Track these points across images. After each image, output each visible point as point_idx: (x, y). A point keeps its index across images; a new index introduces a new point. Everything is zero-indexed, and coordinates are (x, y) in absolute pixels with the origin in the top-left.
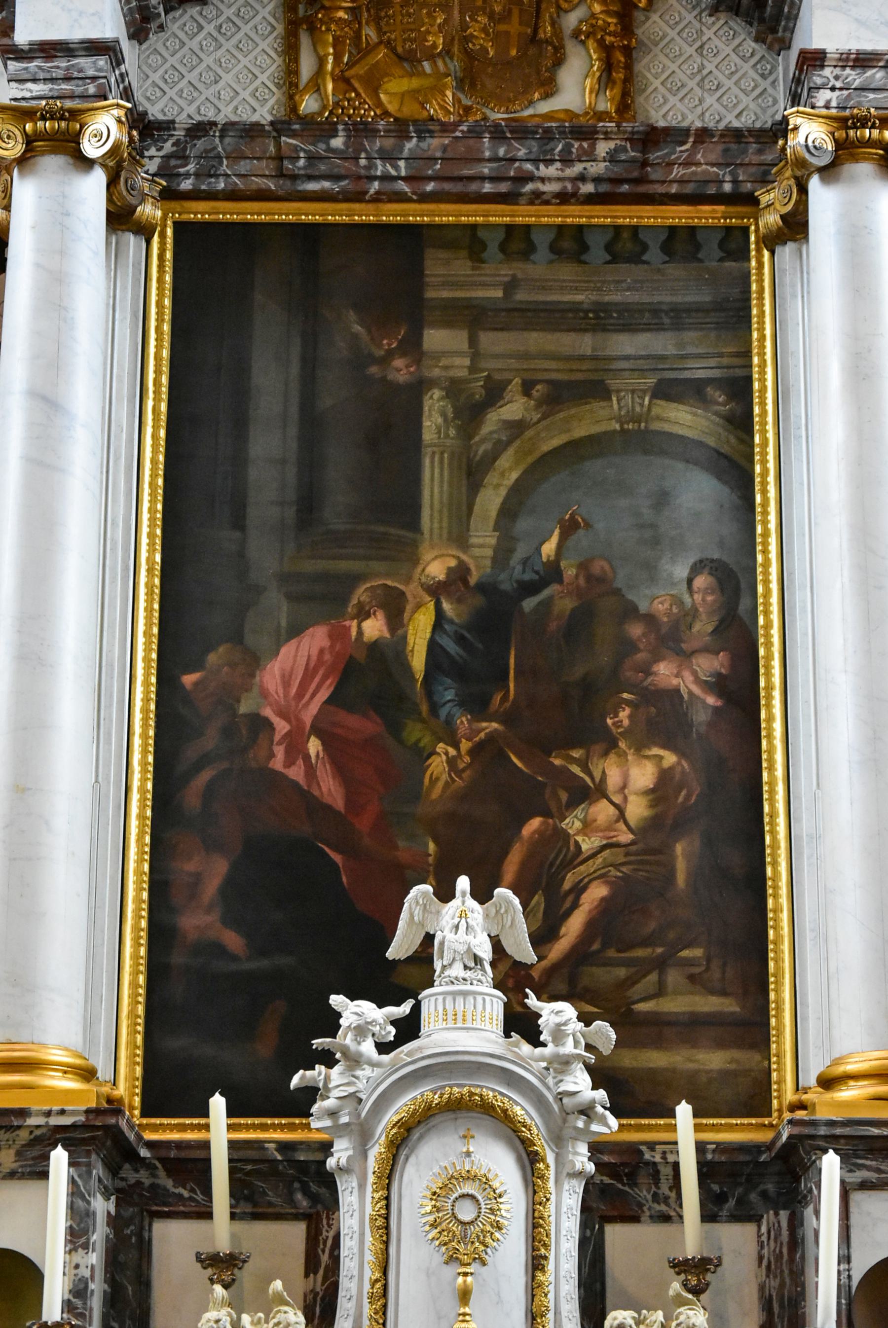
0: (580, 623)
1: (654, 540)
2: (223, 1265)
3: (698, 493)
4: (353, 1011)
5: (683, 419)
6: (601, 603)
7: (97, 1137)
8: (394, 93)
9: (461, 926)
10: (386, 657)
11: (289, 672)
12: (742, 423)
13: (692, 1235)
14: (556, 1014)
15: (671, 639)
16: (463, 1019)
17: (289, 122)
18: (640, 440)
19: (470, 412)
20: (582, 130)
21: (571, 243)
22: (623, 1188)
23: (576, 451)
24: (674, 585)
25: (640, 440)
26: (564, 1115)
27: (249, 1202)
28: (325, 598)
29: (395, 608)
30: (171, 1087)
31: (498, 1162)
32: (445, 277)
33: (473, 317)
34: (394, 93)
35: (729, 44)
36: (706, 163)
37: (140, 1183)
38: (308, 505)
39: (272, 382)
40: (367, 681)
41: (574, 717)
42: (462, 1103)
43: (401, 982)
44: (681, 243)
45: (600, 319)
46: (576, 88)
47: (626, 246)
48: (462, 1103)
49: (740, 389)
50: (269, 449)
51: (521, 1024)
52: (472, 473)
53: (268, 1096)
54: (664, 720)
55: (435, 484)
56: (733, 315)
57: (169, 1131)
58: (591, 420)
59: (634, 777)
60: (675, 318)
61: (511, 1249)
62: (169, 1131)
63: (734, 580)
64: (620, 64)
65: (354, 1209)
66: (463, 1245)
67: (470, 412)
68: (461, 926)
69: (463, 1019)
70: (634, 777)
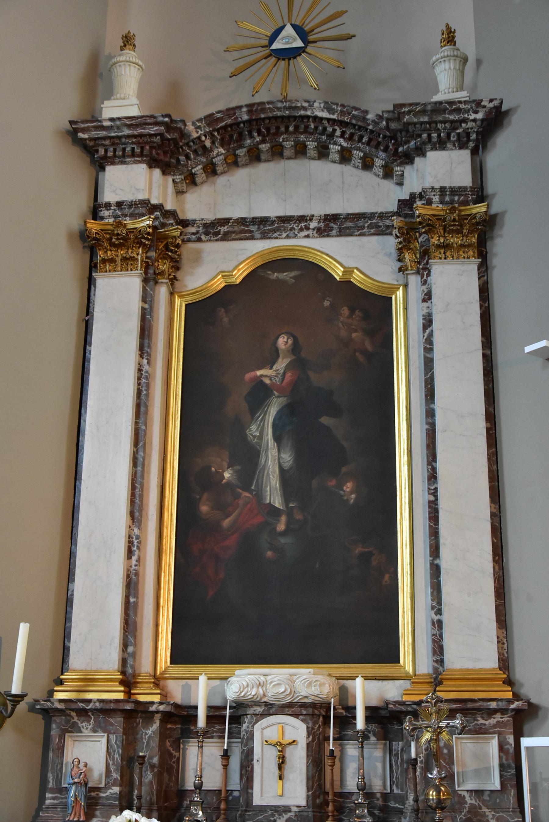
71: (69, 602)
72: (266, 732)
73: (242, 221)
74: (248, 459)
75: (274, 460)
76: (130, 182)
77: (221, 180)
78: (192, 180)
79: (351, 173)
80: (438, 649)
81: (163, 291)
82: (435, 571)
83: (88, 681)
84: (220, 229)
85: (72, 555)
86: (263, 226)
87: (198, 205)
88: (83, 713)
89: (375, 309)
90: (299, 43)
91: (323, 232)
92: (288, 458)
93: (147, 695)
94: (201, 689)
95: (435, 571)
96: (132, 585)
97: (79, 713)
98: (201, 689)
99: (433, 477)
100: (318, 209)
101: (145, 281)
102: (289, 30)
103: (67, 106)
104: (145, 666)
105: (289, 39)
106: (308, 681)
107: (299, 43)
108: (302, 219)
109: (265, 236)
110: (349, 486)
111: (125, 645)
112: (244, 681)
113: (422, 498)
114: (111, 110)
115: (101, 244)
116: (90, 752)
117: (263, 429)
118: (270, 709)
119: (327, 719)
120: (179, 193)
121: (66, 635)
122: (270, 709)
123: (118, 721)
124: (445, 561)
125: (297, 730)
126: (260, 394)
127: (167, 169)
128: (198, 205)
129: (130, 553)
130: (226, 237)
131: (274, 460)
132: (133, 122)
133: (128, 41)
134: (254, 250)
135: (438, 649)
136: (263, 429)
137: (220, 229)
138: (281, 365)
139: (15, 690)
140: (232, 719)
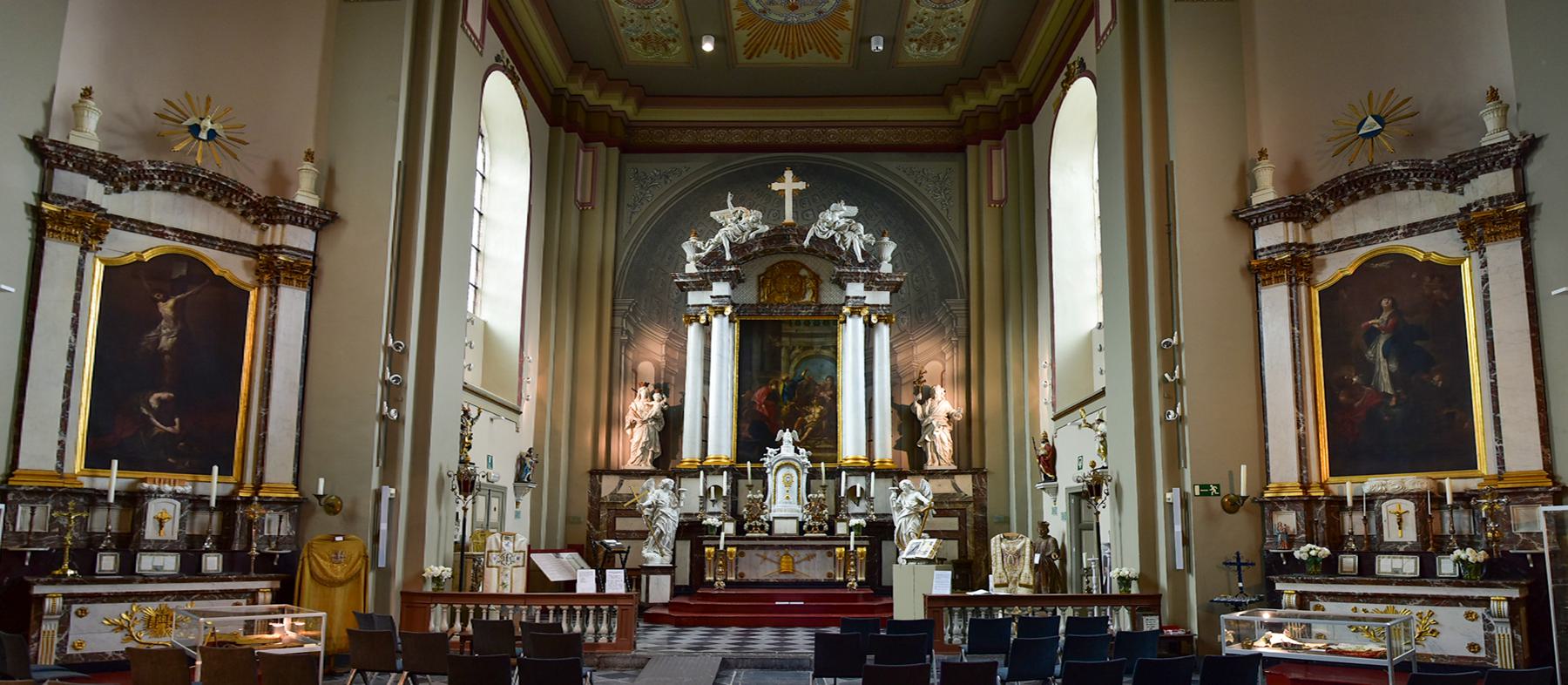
0: (807, 387)
1: (821, 373)
2: (750, 487)
3: (829, 364)
4: (770, 450)
5: (826, 352)
6: (811, 382)
7: (730, 469)
8: (777, 299)
9: (787, 436)
10: (777, 390)
11: (759, 394)
12: (836, 353)
13: (824, 482)
14: (802, 450)
15: (823, 389)
16: (787, 450)
17: (759, 303)
18: (819, 356)
19: (790, 352)
20: (809, 305)
21: (807, 323)
22: (813, 474)
23: (808, 358)
24: (824, 380)
25: (819, 356)
26: (803, 465)
27: (753, 477)
28: (766, 382)
29: (777, 384)
30: (740, 458)
31: (794, 472)
32: (786, 329)
33: (790, 335)
34: (777, 299)
35: (835, 289)
36: (830, 310)
37: (736, 474)
38: (762, 367)
39: (756, 347)
40: (772, 396)
41: (807, 402)
42: (788, 464)
43: (778, 445)
44: (826, 323)
45: (812, 336)
46: (808, 297)
47: (817, 323)
48: (788, 464)
49: (836, 347)
50: (756, 357)
51: (797, 451)
52: (790, 362)
53: (755, 461)
54: (822, 402)
55: (783, 364)
56: (836, 335)
57: (741, 466)
58: (811, 353)
59: (816, 411)
60: (825, 335)
61: (795, 485)
62: (741, 466)
63: (834, 379)
64: (816, 294)
65: (770, 479)
66: (788, 484)
67: (790, 352)
68: (787, 436)
69: (787, 450)
70: (816, 411)
71: (1267, 451)
72: (1389, 508)
73: (1351, 238)
74: (1369, 370)
75: (1384, 370)
76: (1270, 236)
77: (1334, 217)
78: (1315, 221)
79: (1425, 194)
80: (1501, 461)
81: (1303, 289)
82: (1497, 421)
83: (1281, 488)
84: (1334, 246)
85: (1265, 429)
86: (1366, 239)
87: (1320, 235)
88: (1282, 503)
89: (1449, 275)
90: (1378, 127)
91: (1405, 235)
92: (1393, 366)
93: (1316, 492)
94: (1348, 488)
95: (1497, 421)
96: (1302, 442)
97: (1277, 503)
98: (1348, 488)
99: (1493, 368)
100: (1403, 221)
101: (1291, 286)
102: (1370, 120)
103: (1229, 201)
104: (1315, 478)
105: (1371, 124)
106: (1413, 481)
107: (1378, 127)
108: (1391, 230)
109: (1367, 244)
110: (1436, 378)
111: (1301, 470)
112: (1372, 484)
113: (1487, 381)
114: (1257, 199)
115: (1260, 272)
116: (1288, 520)
117: (1377, 352)
118: (1390, 496)
119: (1429, 504)
120: (1307, 229)
121: (1268, 467)
122: (1390, 496)
123: (1301, 505)
124: (1502, 414)
125: (1409, 506)
126: (1372, 334)
127: (1295, 221)
128: (1320, 235)
129: (1298, 426)
130: (1341, 249)
131: (1384, 370)
132: (1271, 203)
133: (1263, 154)
134: (1363, 251)
135: (1501, 461)
136: (1377, 352)
137: (1334, 246)
138: (1385, 316)
139: (1243, 494)
140: (1369, 502)
